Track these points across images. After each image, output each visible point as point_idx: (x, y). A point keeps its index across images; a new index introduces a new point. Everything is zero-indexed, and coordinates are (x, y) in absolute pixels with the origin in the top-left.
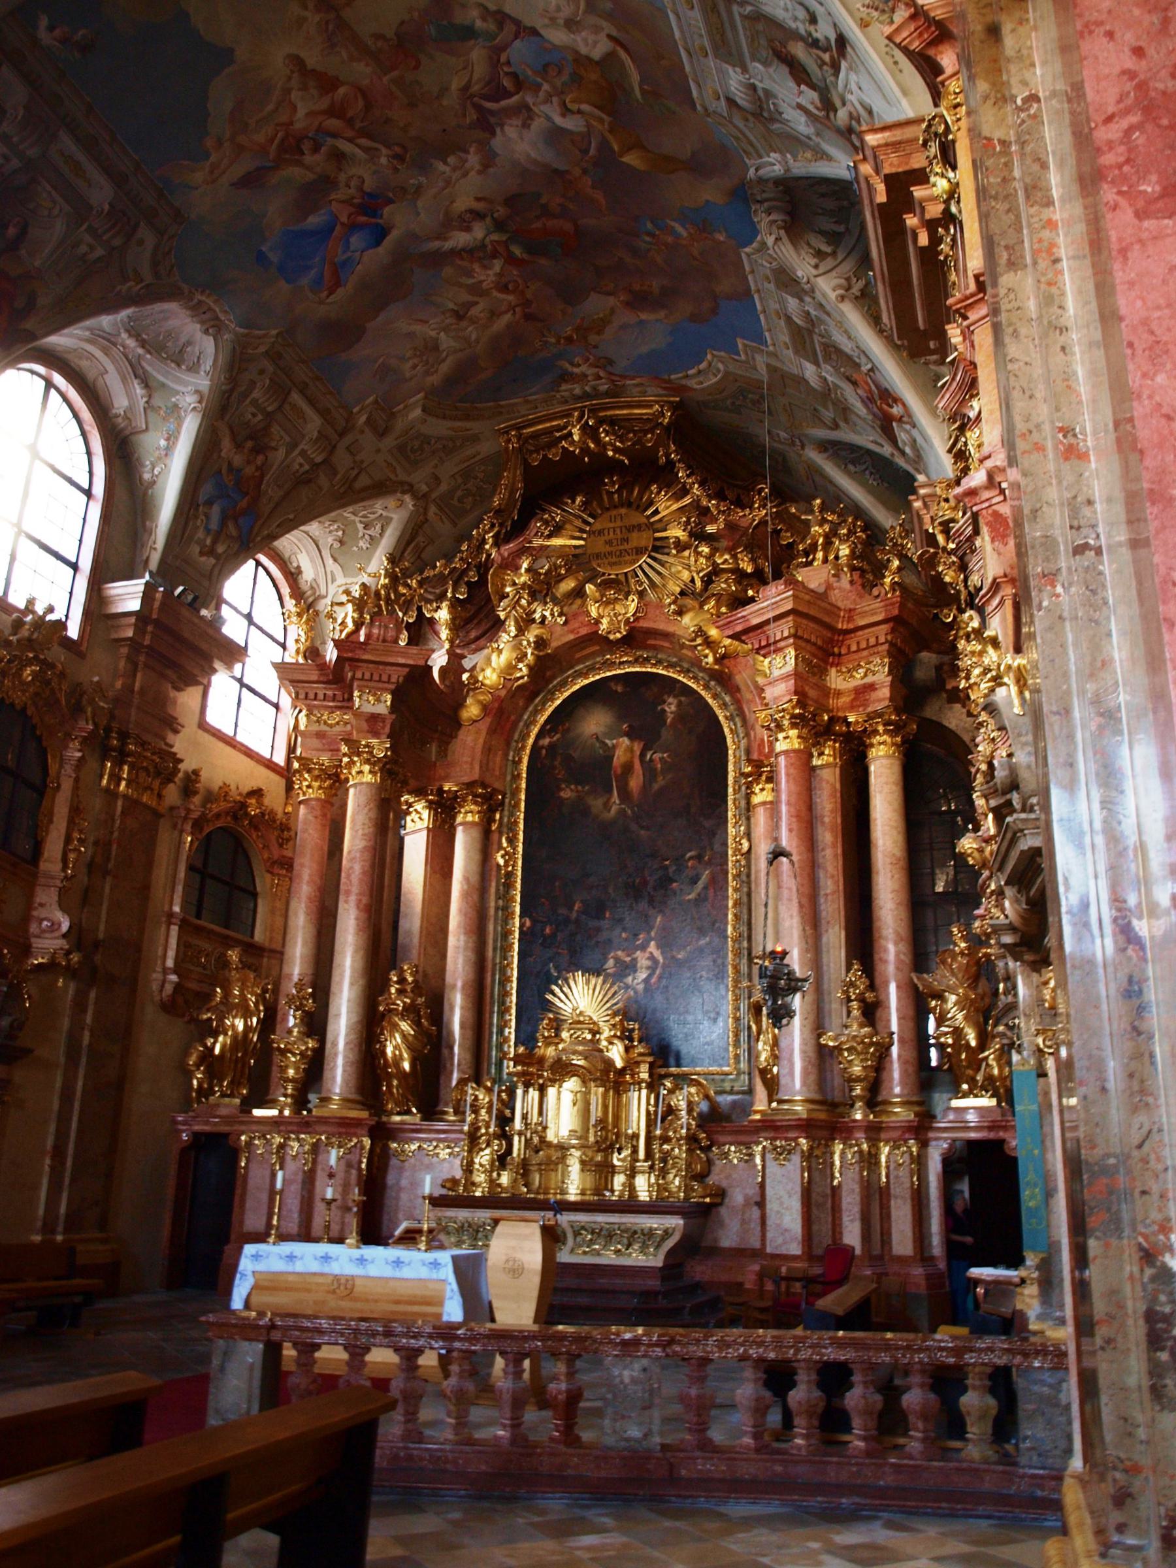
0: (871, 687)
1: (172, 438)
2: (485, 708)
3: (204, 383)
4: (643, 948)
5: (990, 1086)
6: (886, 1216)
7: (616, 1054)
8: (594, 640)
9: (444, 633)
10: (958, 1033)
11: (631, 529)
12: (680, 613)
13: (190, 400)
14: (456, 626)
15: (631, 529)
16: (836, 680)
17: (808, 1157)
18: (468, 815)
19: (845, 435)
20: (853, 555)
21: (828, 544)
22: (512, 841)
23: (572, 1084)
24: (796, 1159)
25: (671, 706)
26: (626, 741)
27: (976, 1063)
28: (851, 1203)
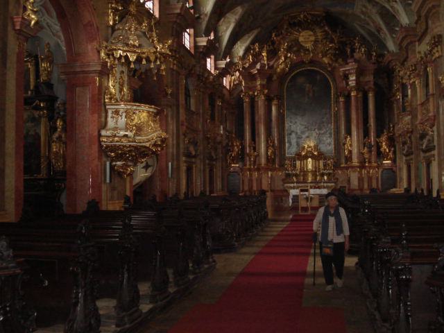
0: (369, 81)
1: (227, 28)
2: (278, 78)
3: (237, 17)
4: (315, 130)
5: (390, 159)
6: (371, 182)
7: (316, 153)
8: (303, 62)
9: (265, 58)
10: (385, 150)
11: (310, 35)
12: (323, 57)
13: (233, 20)
14: (267, 57)
15: (310, 35)
16: (361, 79)
17: (359, 172)
18: (275, 102)
19: (368, 27)
20: (365, 51)
21: (359, 48)
22: (284, 107)
23: (310, 160)
24: (357, 173)
25: (318, 77)
26: (308, 85)
27: (388, 155)
28: (366, 180)
